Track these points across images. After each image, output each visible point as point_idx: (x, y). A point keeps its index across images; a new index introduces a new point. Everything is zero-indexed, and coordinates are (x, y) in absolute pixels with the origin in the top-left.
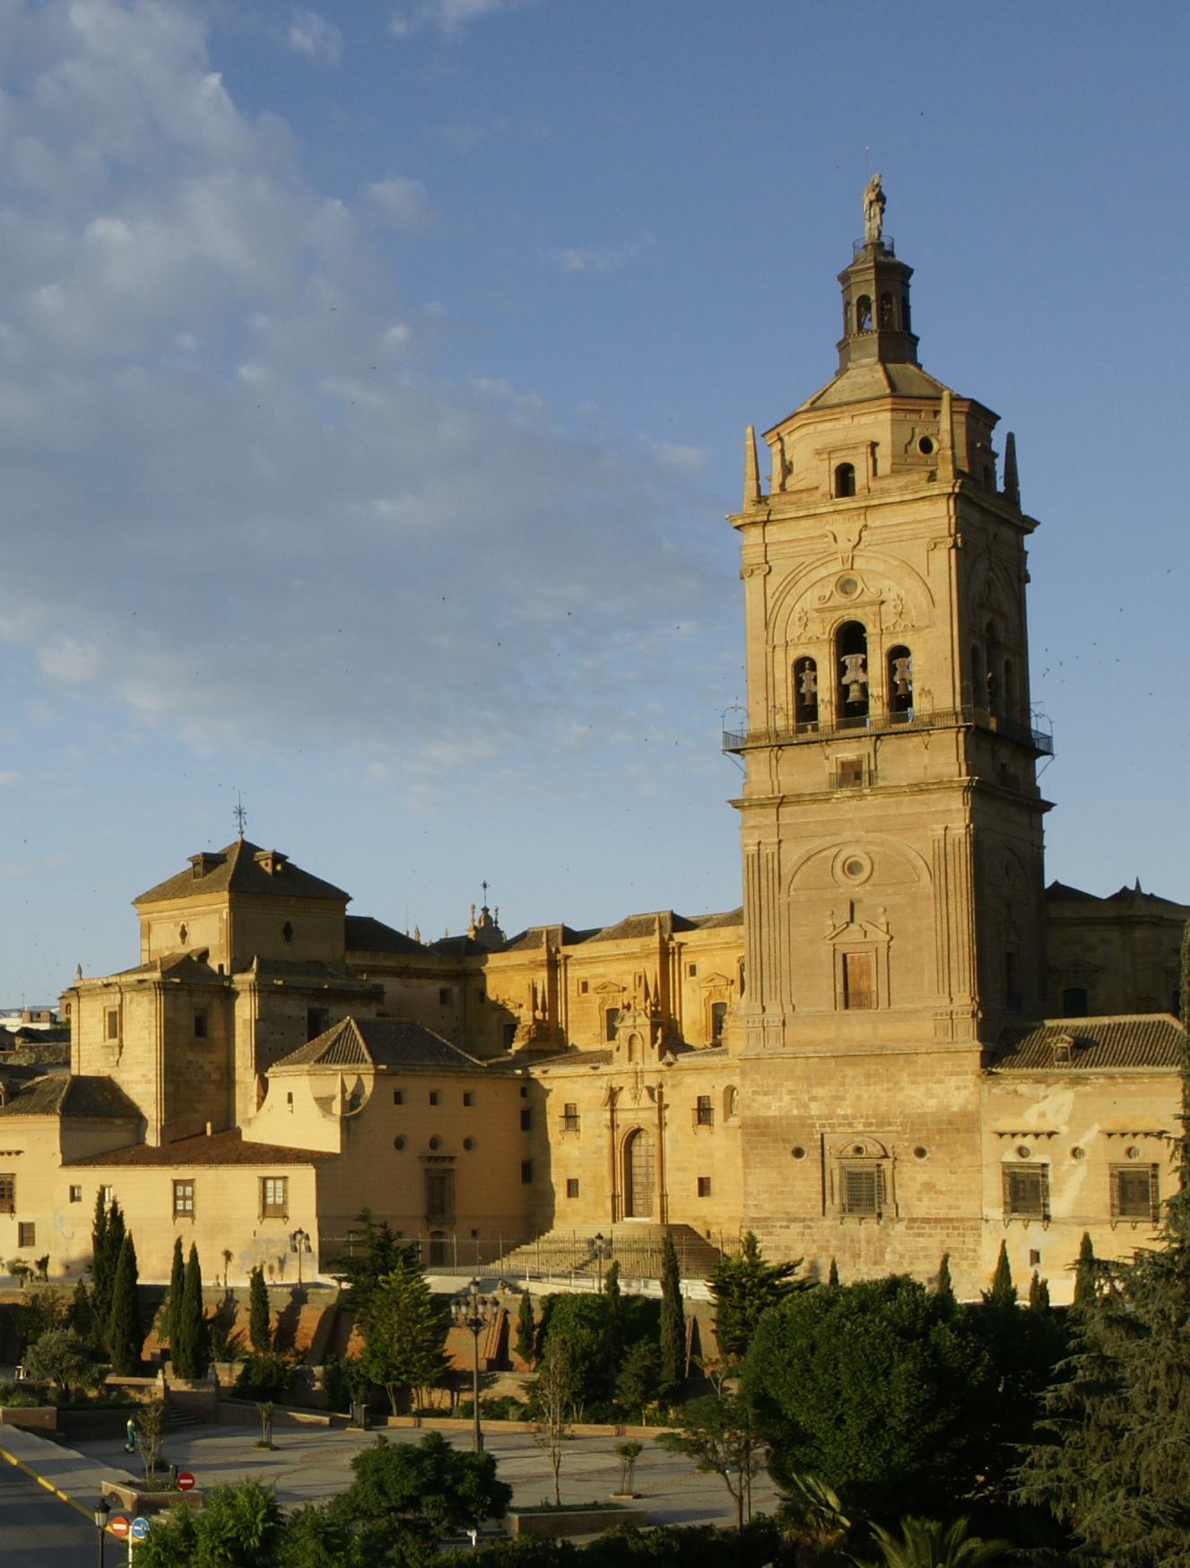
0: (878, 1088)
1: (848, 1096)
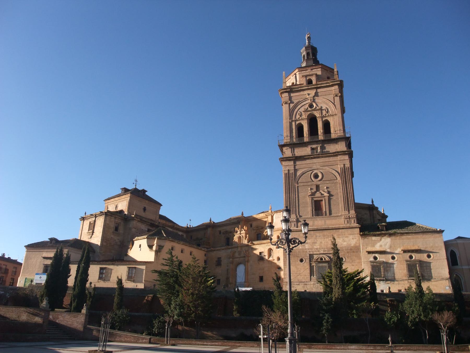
0: (327, 240)
1: (318, 242)
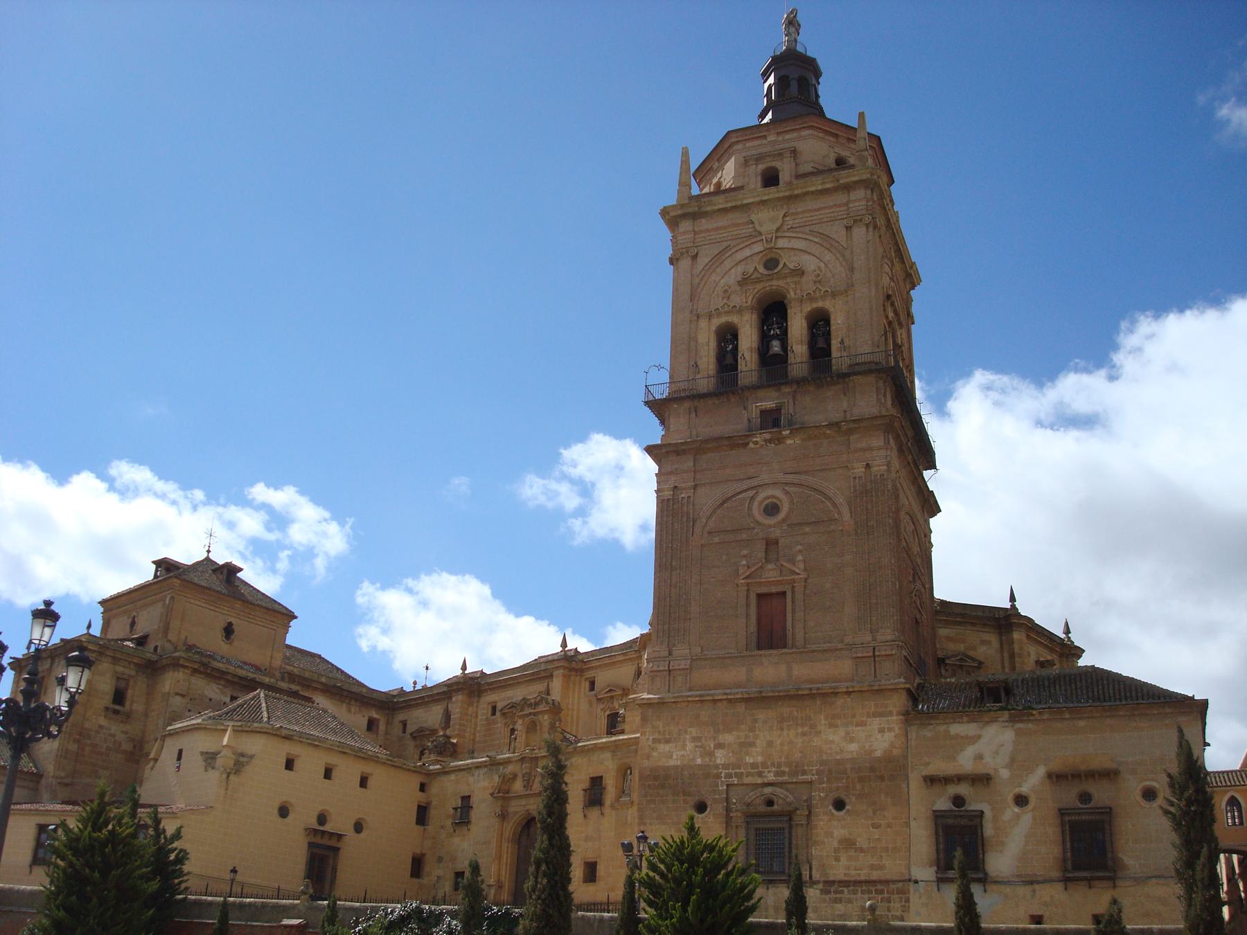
0: (792, 732)
1: (758, 741)
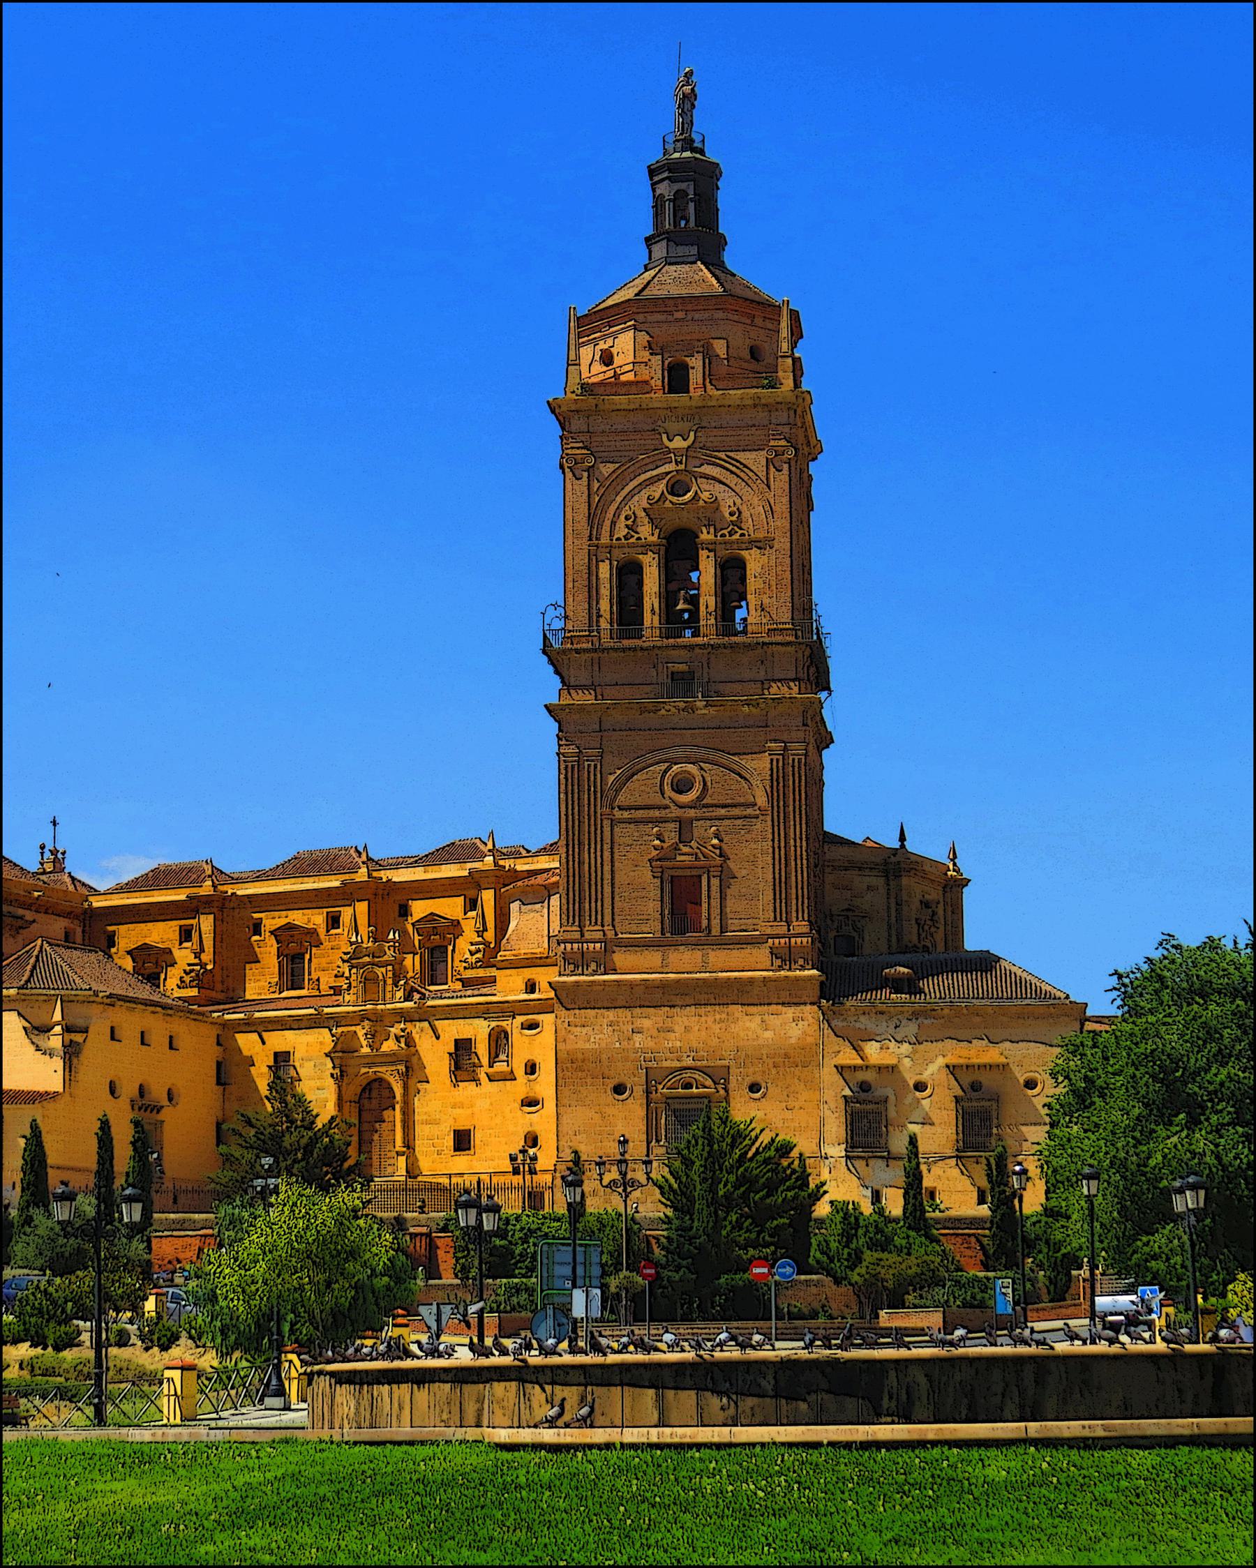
0: (710, 1019)
